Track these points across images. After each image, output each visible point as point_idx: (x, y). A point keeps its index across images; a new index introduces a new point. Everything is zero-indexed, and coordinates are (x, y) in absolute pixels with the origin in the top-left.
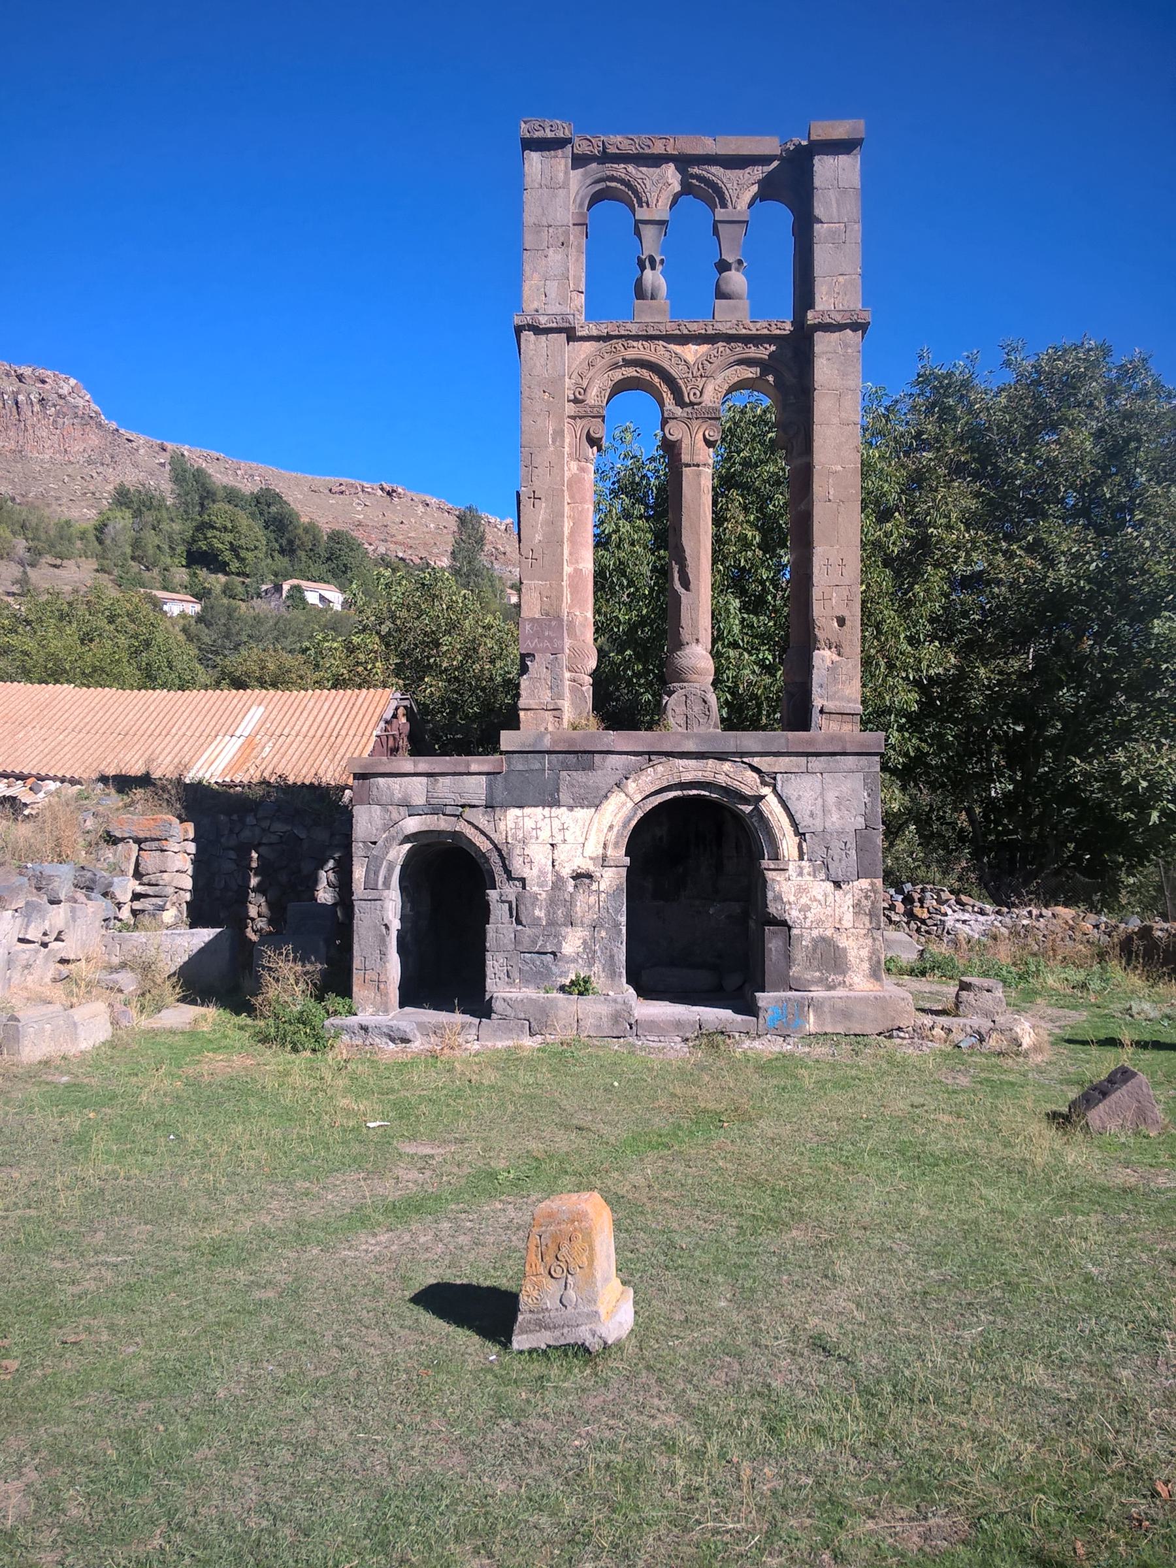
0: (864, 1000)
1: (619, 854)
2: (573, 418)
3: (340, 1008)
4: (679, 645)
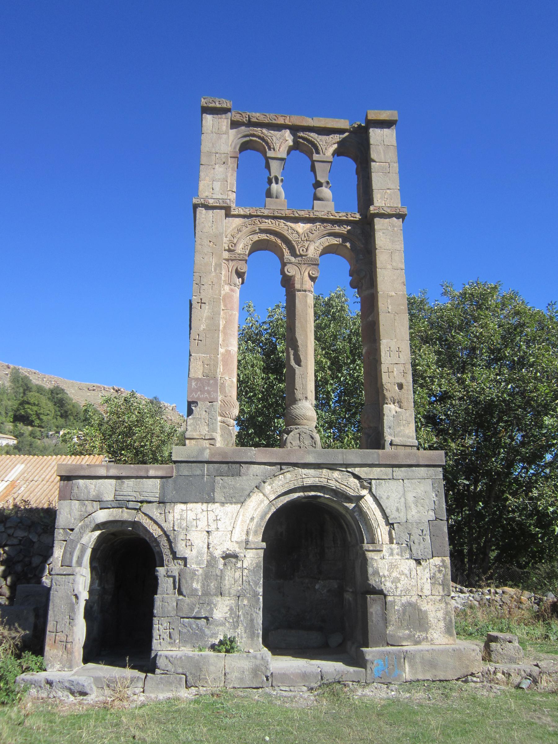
0: (442, 652)
1: (257, 539)
2: (227, 260)
3: (33, 666)
4: (294, 401)
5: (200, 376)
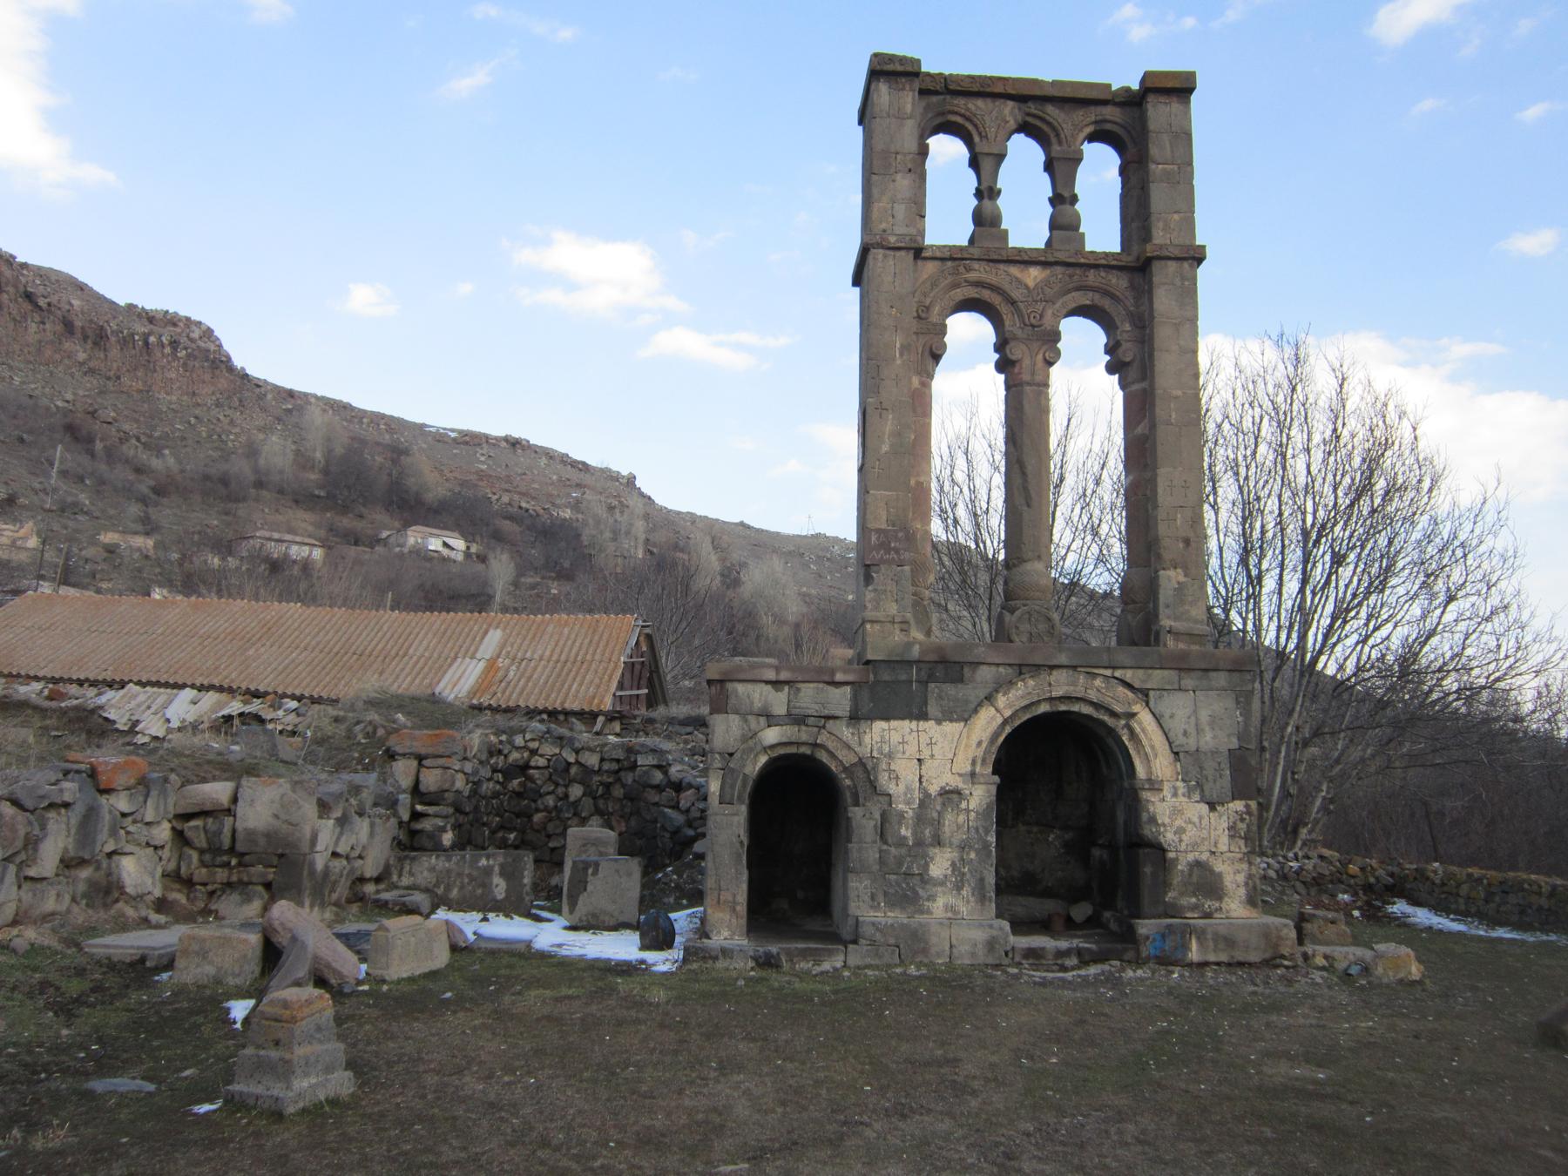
5: (884, 526)
